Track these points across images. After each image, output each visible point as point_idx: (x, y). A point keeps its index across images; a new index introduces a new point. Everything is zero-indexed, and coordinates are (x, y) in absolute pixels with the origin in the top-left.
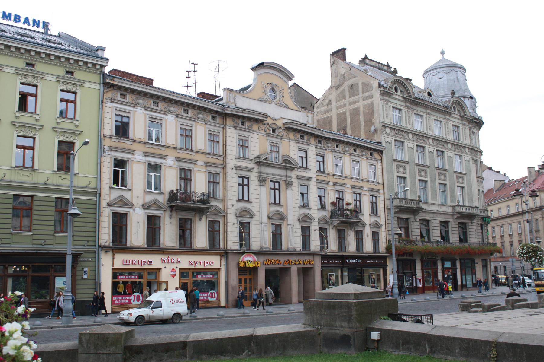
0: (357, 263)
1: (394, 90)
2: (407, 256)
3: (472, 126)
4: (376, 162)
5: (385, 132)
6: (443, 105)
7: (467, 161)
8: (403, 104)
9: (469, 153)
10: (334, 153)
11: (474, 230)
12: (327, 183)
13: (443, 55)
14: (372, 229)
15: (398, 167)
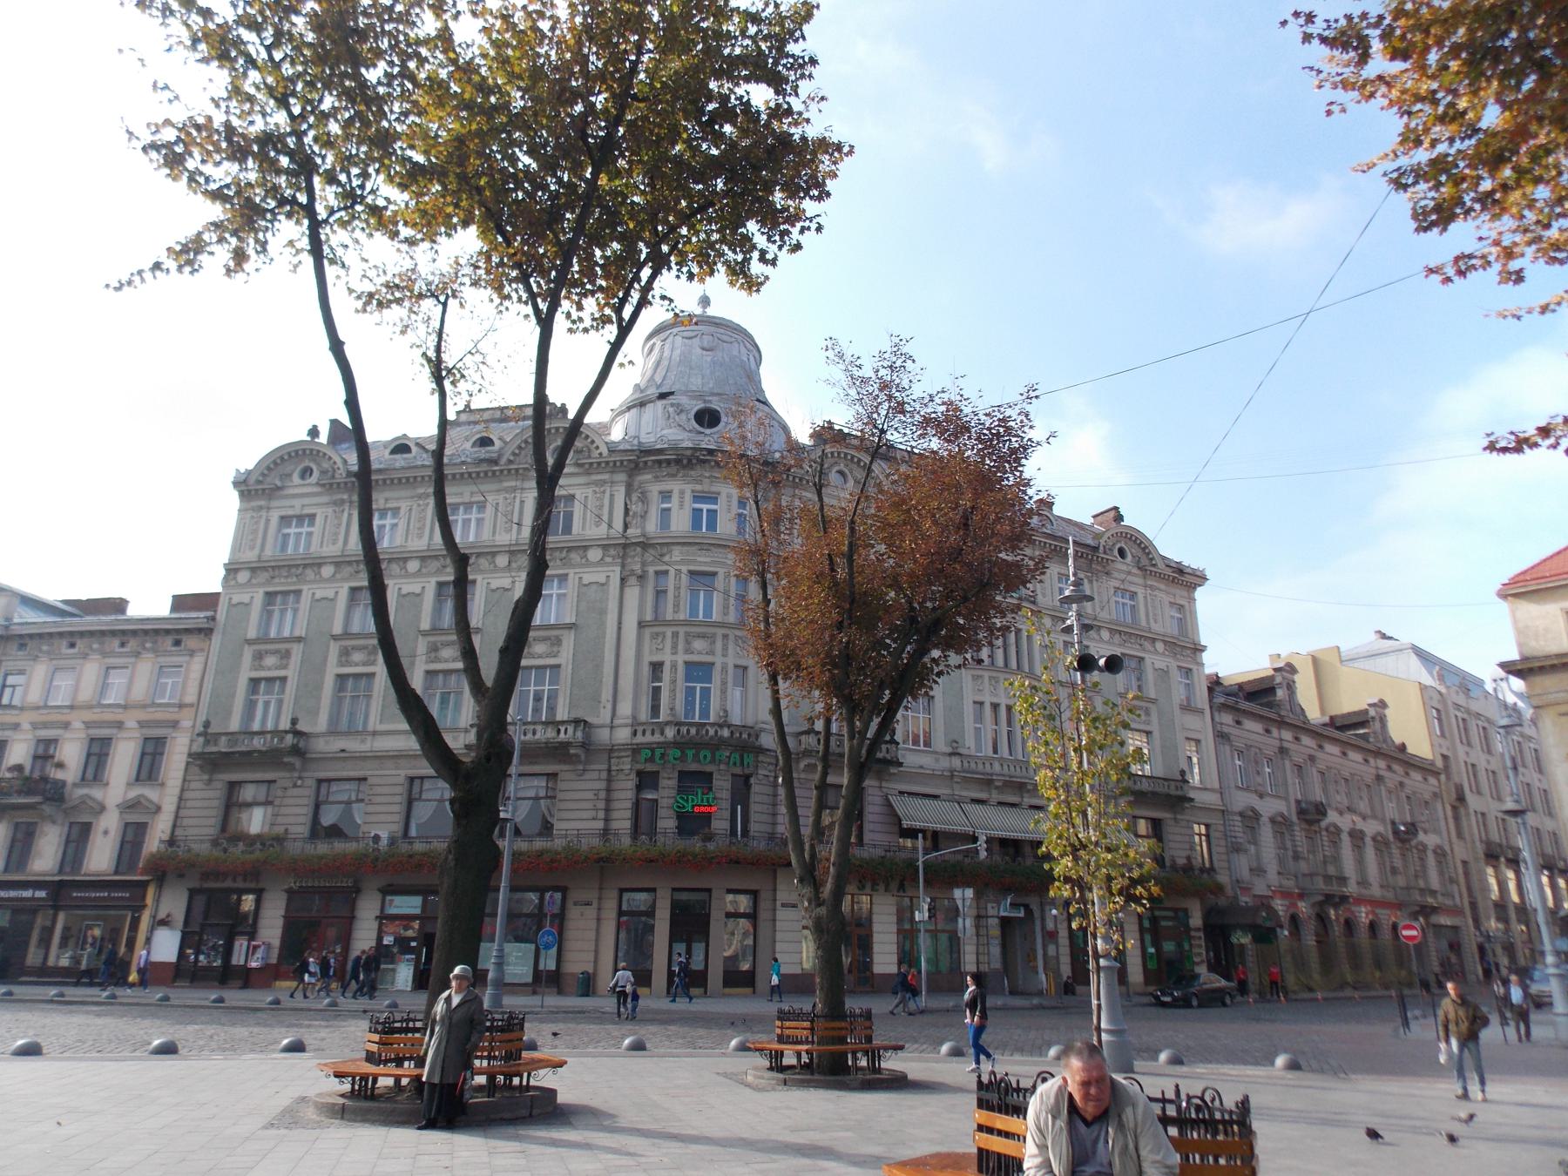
0: (33, 899)
1: (296, 479)
2: (234, 880)
3: (656, 477)
4: (187, 658)
5: (233, 583)
6: (469, 460)
7: (594, 587)
8: (325, 499)
9: (608, 560)
10: (55, 662)
11: (590, 795)
12: (16, 727)
13: (704, 307)
14: (125, 816)
15: (259, 656)
